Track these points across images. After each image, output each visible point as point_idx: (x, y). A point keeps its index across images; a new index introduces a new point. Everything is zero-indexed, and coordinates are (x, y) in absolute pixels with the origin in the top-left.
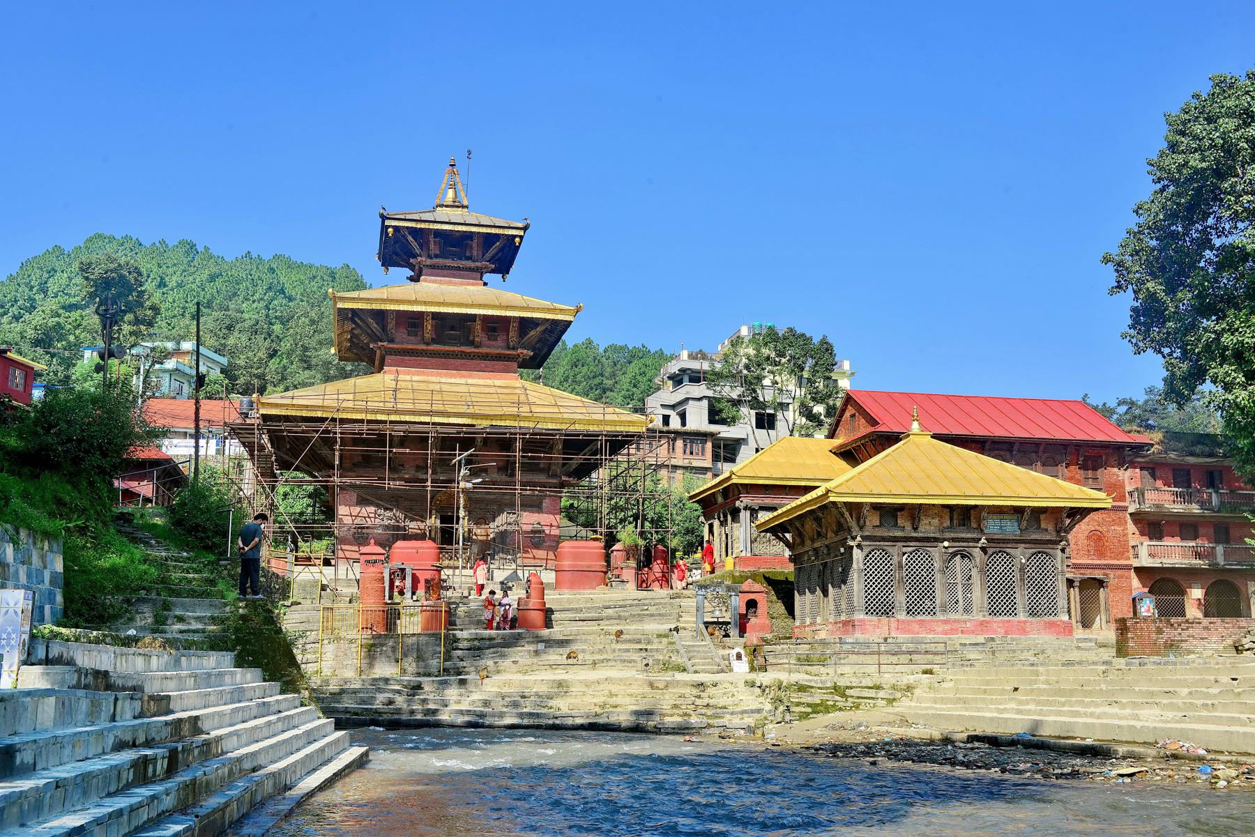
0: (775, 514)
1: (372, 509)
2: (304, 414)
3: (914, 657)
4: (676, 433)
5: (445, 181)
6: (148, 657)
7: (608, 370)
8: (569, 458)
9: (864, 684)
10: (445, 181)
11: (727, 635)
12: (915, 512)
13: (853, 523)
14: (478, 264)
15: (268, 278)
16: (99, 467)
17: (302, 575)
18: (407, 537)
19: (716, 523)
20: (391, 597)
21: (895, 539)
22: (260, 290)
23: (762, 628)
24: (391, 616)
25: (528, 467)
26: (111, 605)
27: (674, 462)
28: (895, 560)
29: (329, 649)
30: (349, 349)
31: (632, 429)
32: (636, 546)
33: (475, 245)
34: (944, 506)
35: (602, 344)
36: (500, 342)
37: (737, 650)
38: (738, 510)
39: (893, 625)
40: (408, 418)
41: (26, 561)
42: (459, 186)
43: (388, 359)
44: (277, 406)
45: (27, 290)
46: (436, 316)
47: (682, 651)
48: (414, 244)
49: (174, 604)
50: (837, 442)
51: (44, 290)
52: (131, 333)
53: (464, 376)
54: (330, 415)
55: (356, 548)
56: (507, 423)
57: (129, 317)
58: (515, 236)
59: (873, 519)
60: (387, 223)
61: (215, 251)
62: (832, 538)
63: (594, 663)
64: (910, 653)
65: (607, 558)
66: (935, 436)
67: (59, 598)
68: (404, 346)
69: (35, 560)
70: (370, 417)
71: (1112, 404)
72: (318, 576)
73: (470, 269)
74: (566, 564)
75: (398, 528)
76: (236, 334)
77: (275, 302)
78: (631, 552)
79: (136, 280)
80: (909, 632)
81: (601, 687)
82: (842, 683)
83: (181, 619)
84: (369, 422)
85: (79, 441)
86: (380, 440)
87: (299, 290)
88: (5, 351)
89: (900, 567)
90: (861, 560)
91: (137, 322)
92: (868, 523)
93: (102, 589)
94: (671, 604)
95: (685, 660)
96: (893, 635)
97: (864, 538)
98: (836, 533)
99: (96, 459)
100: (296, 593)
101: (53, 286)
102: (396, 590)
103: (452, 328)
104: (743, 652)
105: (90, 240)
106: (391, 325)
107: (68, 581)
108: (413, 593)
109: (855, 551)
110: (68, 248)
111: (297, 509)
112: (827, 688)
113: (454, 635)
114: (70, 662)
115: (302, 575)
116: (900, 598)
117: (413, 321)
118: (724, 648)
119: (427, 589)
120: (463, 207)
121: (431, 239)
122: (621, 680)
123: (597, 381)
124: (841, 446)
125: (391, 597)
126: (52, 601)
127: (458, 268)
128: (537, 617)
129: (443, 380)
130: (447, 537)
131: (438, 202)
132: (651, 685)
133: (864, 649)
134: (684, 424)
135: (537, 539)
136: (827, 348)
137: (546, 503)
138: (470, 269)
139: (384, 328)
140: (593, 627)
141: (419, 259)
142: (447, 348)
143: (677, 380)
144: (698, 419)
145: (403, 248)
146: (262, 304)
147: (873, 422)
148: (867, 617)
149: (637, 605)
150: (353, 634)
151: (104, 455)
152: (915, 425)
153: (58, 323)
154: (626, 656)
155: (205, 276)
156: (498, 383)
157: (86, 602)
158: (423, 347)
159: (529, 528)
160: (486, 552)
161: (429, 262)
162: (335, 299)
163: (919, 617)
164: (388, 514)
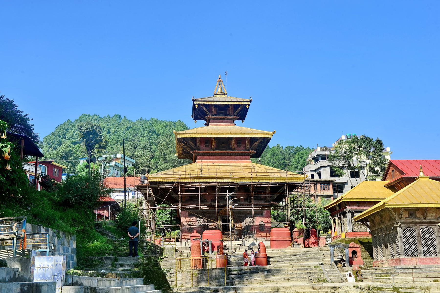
0: (362, 214)
1: (194, 218)
2: (166, 181)
3: (429, 274)
4: (318, 182)
5: (217, 84)
6: (110, 281)
7: (287, 157)
8: (274, 193)
9: (407, 287)
10: (217, 84)
11: (344, 266)
12: (424, 211)
13: (396, 217)
14: (232, 117)
15: (149, 127)
16: (88, 206)
17: (167, 246)
18: (208, 229)
19: (337, 219)
20: (203, 254)
21: (416, 223)
22: (146, 132)
23: (359, 263)
24: (204, 262)
25: (257, 198)
26: (95, 261)
27: (317, 193)
28: (417, 232)
29: (180, 276)
30: (182, 154)
31: (299, 181)
32: (303, 229)
33: (230, 110)
34: (437, 208)
35: (284, 146)
36: (242, 148)
37: (349, 272)
38: (346, 213)
39: (418, 260)
40: (207, 181)
42: (223, 86)
43: (198, 157)
44: (155, 178)
45: (58, 137)
46: (216, 138)
47: (325, 273)
49: (119, 259)
50: (387, 182)
51: (64, 137)
52: (98, 152)
53: (228, 163)
54: (176, 181)
55: (189, 234)
56: (247, 181)
57: (97, 146)
58: (247, 105)
59: (406, 215)
60: (195, 103)
61: (128, 118)
62: (387, 223)
63: (288, 279)
64: (427, 273)
65: (291, 234)
66: (431, 178)
67: (75, 258)
68: (204, 151)
69: (66, 243)
70: (192, 181)
72: (174, 246)
73: (229, 119)
74: (274, 238)
75: (205, 225)
76: (138, 150)
77: (152, 137)
78: (301, 232)
79: (99, 131)
80: (426, 263)
81: (292, 289)
82: (397, 286)
83: (122, 265)
84: (192, 183)
85: (81, 196)
86: (196, 190)
88: (51, 162)
89: (419, 235)
90: (401, 233)
91: (100, 147)
92: (403, 216)
93: (91, 254)
94: (320, 253)
95: (327, 277)
96: (418, 265)
97: (402, 223)
98: (389, 221)
99: (87, 202)
100: (165, 254)
101: (68, 136)
102: (205, 251)
103: (223, 143)
104: (352, 273)
105: (81, 117)
106: (199, 143)
107: (78, 251)
108: (212, 252)
109: (398, 228)
110: (73, 120)
111: (164, 219)
112: (390, 288)
113: (230, 269)
114: (81, 284)
115: (167, 246)
116: (420, 248)
117: (207, 141)
118: (343, 271)
119: (218, 250)
120: (225, 94)
121: (213, 108)
122: (300, 286)
123: (282, 161)
124: (389, 184)
125: (203, 254)
126: (72, 260)
127: (224, 119)
128: (264, 260)
129: (220, 164)
130: (225, 228)
131: (215, 93)
132: (313, 288)
133: (405, 271)
134: (320, 177)
135: (262, 229)
136: (379, 143)
137: (265, 213)
138: (229, 119)
139: (196, 145)
140: (287, 264)
141: (208, 116)
142: (221, 151)
143: (316, 159)
144: (326, 175)
145: (202, 112)
146: (147, 138)
147: (402, 173)
148: (406, 257)
149: (305, 254)
150: (189, 269)
151: (90, 201)
152: (421, 174)
153: (70, 150)
154: (302, 276)
155: (125, 128)
156: (242, 164)
157: (85, 260)
158: (212, 151)
159: (258, 224)
160: (241, 234)
161: (212, 117)
162: (176, 134)
163: (429, 257)
164: (201, 220)
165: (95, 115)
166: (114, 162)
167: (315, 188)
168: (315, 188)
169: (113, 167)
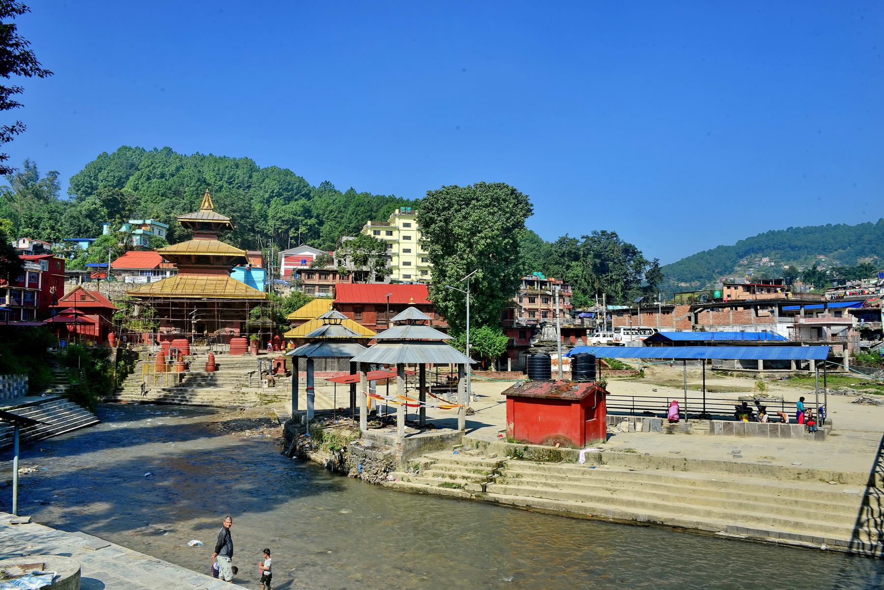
22: (194, 182)
41: (16, 381)
51: (96, 179)
57: (118, 216)
65: (248, 343)
69: (19, 380)
71: (578, 238)
76: (174, 211)
87: (213, 180)
101: (100, 178)
105: (119, 150)
110: (110, 153)
123: (368, 214)
144: (350, 265)
146: (194, 188)
155: (173, 168)
165: (137, 148)
166: (143, 228)
167: (334, 278)
168: (334, 278)
169: (140, 235)
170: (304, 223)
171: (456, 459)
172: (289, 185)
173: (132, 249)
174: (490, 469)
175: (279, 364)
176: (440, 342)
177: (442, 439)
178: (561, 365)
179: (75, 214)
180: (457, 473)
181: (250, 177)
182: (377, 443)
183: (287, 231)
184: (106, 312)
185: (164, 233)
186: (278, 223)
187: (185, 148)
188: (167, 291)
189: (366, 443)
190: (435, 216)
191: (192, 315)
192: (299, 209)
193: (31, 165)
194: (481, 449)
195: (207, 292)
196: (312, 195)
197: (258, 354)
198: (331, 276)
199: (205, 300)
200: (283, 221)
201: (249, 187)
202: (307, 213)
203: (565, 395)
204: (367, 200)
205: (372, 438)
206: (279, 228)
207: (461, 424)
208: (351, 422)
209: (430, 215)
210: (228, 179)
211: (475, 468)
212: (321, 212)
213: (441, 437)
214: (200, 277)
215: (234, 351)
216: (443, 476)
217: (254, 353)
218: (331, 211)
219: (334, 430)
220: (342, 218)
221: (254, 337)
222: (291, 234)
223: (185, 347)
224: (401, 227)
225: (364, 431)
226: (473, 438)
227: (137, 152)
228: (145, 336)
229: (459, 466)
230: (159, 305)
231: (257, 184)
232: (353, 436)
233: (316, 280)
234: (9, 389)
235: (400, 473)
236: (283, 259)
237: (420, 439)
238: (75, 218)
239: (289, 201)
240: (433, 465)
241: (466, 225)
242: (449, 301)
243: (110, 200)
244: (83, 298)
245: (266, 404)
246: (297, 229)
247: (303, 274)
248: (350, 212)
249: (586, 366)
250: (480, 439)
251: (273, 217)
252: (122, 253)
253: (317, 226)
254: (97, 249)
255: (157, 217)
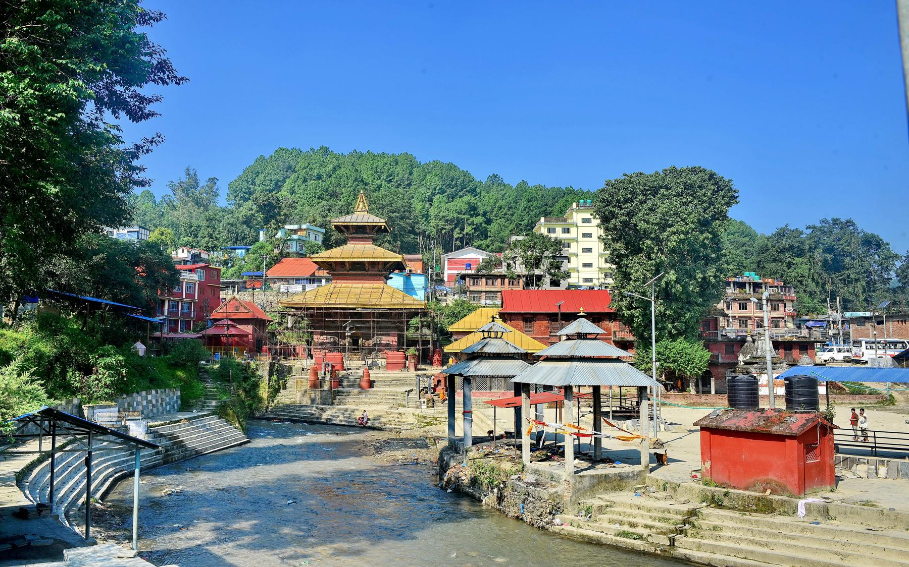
7: (550, 203)
15: (354, 175)
22: (351, 181)
48: (345, 230)
51: (253, 183)
52: (275, 229)
57: (274, 221)
69: (171, 395)
84: (318, 308)
87: (371, 179)
101: (258, 181)
105: (277, 151)
107: (182, 397)
110: (267, 157)
123: (544, 208)
146: (352, 189)
155: (330, 168)
156: (375, 286)
167: (503, 283)
168: (503, 283)
169: (297, 240)
170: (469, 222)
171: (638, 503)
172: (452, 180)
173: (287, 255)
174: (680, 517)
175: (439, 381)
176: (618, 360)
177: (621, 477)
178: (771, 389)
179: (232, 221)
180: (638, 520)
181: (411, 174)
182: (542, 480)
183: (452, 230)
184: (260, 323)
185: (320, 239)
186: (442, 223)
187: (342, 147)
188: (321, 301)
189: (529, 478)
190: (616, 210)
191: (345, 327)
192: (464, 207)
193: (192, 172)
194: (670, 491)
195: (361, 301)
196: (478, 190)
197: (417, 370)
198: (499, 280)
199: (359, 310)
200: (447, 221)
201: (409, 185)
202: (473, 210)
203: (776, 429)
204: (540, 193)
205: (536, 472)
206: (442, 229)
207: (645, 459)
208: (513, 452)
209: (610, 208)
210: (388, 177)
211: (660, 515)
212: (489, 209)
213: (619, 475)
214: (354, 285)
215: (390, 366)
216: (621, 523)
217: (412, 369)
218: (501, 208)
219: (494, 461)
220: (512, 215)
221: (412, 351)
222: (456, 235)
223: (339, 361)
224: (580, 223)
225: (527, 463)
226: (659, 478)
227: (294, 154)
228: (299, 350)
229: (641, 512)
230: (312, 316)
231: (418, 181)
232: (514, 469)
233: (482, 286)
234: (162, 404)
235: (569, 516)
236: (446, 263)
237: (593, 476)
238: (232, 225)
239: (453, 198)
240: (609, 509)
241: (653, 218)
242: (636, 308)
243: (265, 205)
244: (237, 308)
245: (424, 426)
246: (462, 229)
247: (468, 279)
248: (521, 208)
249: (801, 392)
250: (668, 480)
251: (436, 217)
252: (277, 260)
253: (484, 225)
254: (253, 256)
255: (314, 221)
